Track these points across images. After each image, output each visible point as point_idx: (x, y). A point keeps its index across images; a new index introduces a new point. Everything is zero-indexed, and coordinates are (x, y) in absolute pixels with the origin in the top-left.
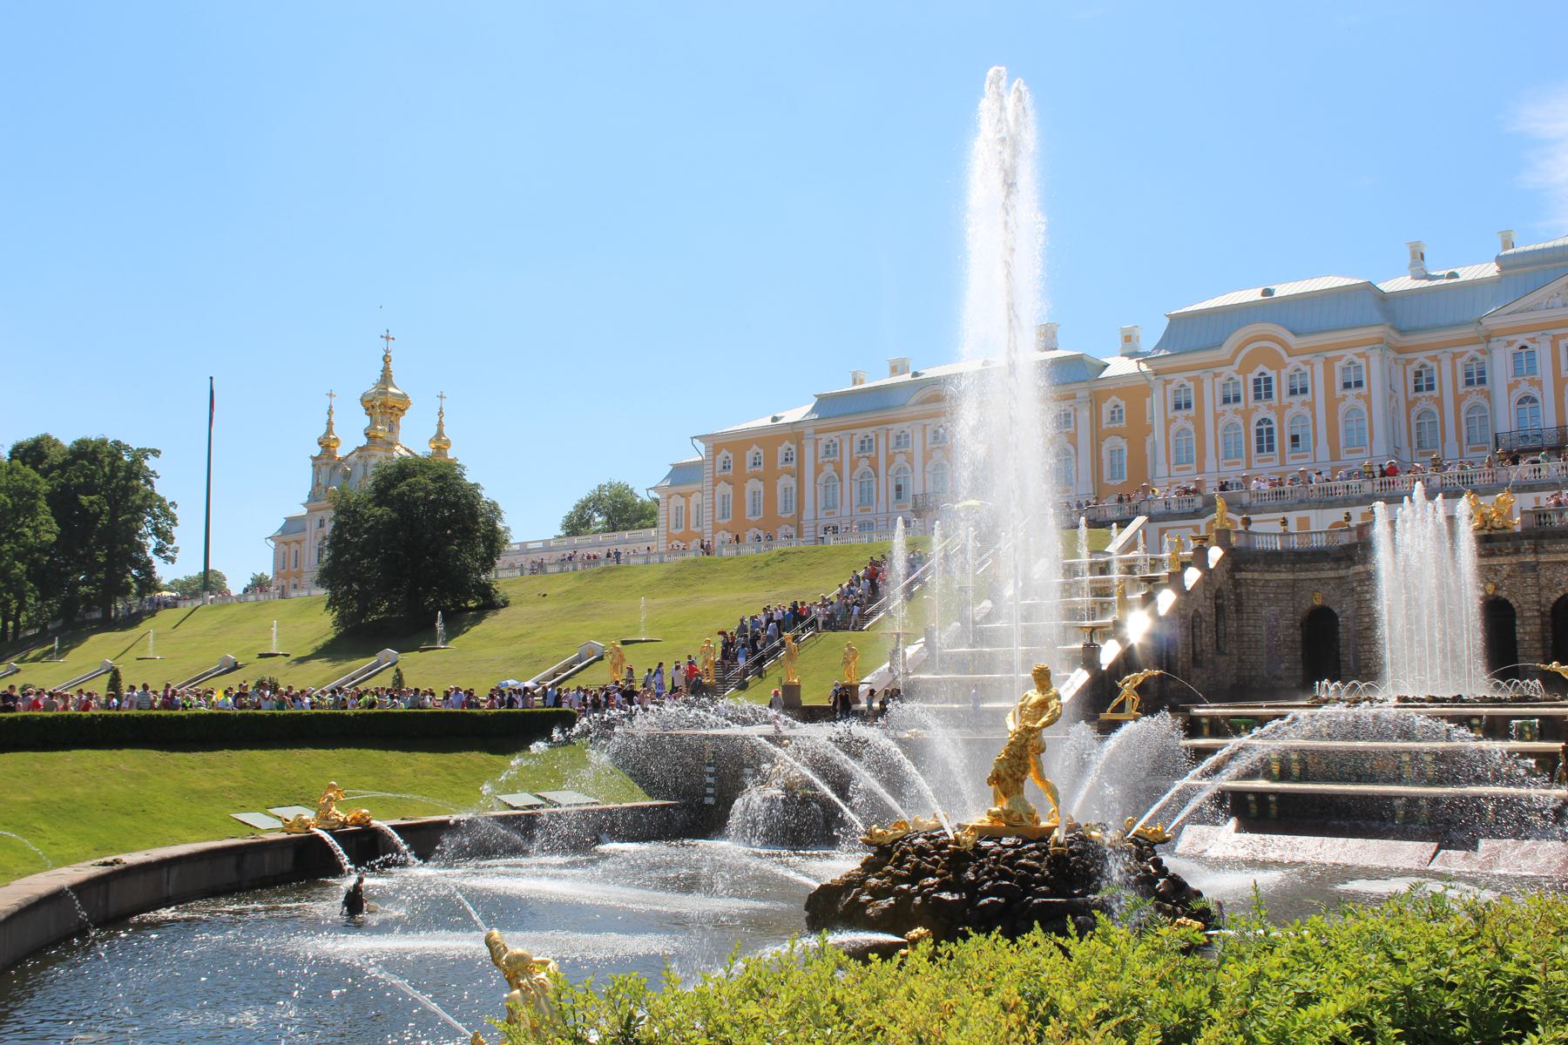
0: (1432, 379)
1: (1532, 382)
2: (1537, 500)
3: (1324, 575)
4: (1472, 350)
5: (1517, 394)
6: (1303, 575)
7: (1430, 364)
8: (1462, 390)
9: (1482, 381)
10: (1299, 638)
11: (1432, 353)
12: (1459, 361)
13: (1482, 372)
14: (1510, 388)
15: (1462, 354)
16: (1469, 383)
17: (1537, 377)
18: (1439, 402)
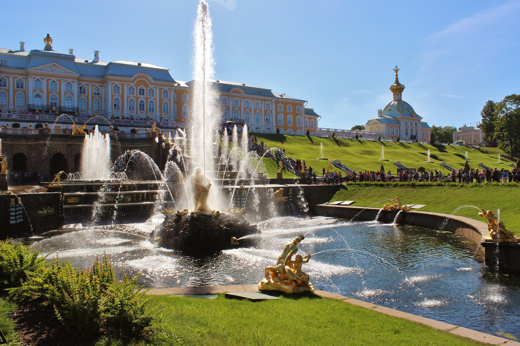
0: (5, 83)
1: (40, 91)
2: (67, 126)
3: (22, 143)
4: (20, 77)
5: (35, 93)
6: (14, 143)
7: (5, 78)
8: (16, 89)
9: (22, 87)
10: (12, 163)
11: (7, 75)
12: (15, 80)
13: (22, 84)
14: (34, 91)
15: (16, 78)
16: (18, 87)
17: (42, 90)
18: (8, 91)
